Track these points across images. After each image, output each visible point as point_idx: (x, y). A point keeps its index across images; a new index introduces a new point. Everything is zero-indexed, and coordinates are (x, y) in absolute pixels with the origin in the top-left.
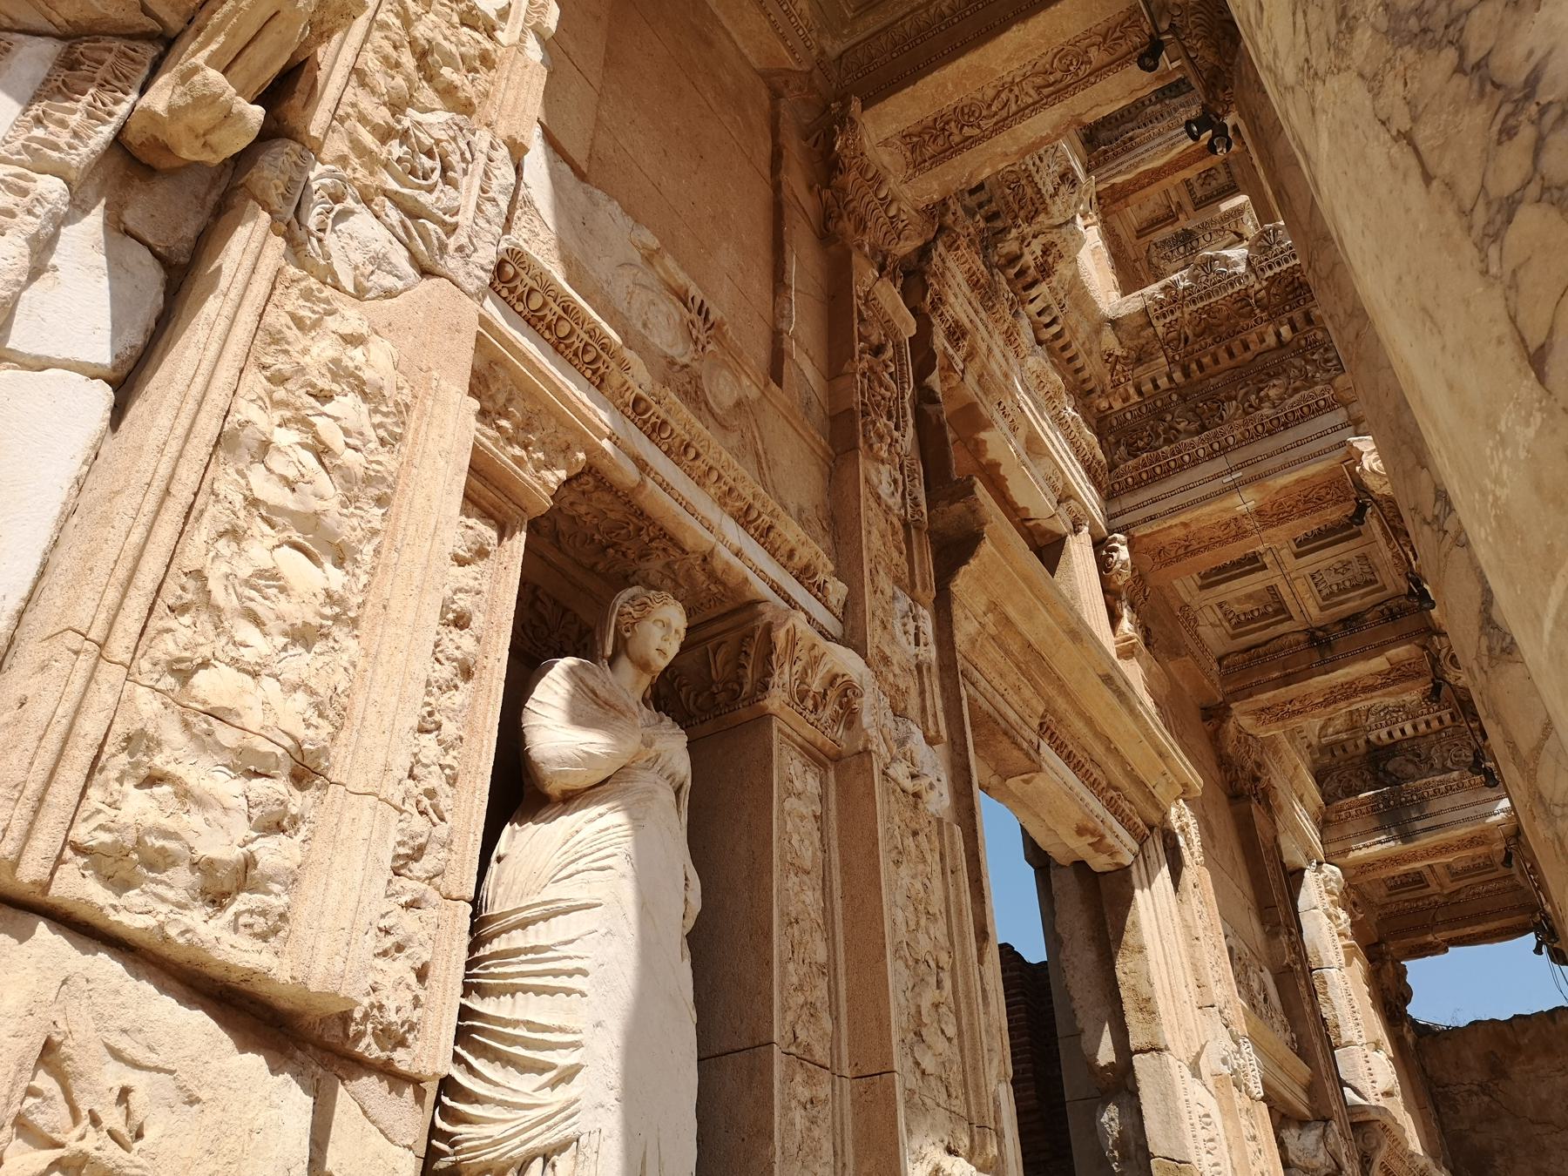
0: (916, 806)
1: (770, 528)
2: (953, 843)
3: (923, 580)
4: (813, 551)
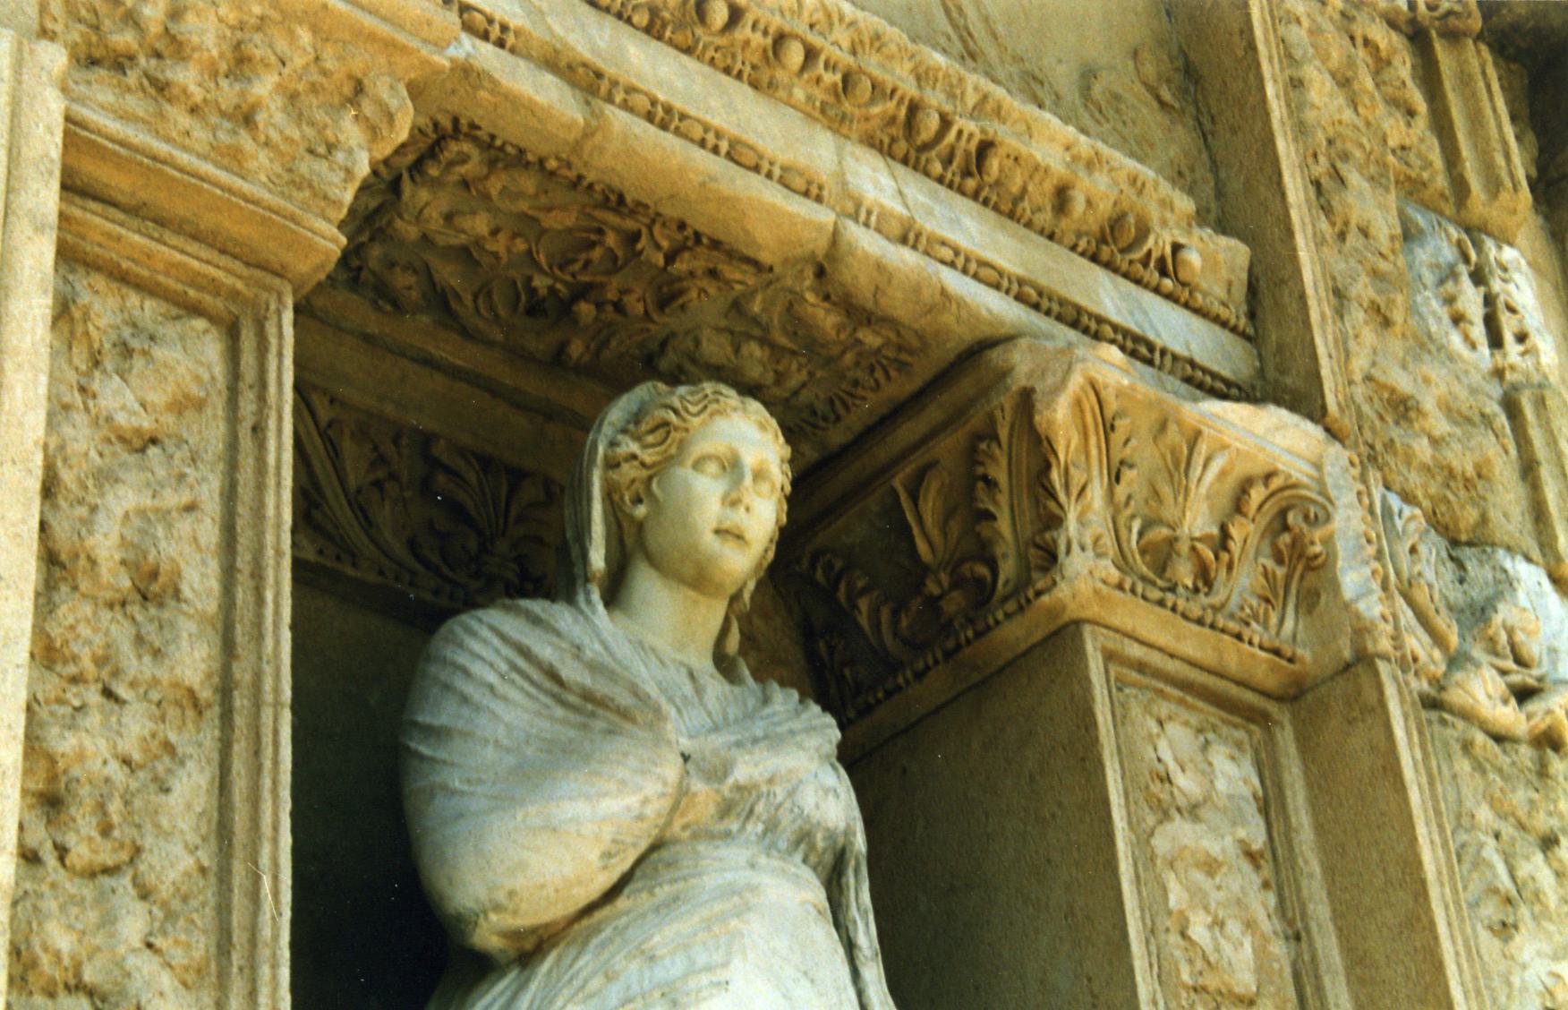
0: (1543, 772)
1: (985, 148)
3: (1488, 170)
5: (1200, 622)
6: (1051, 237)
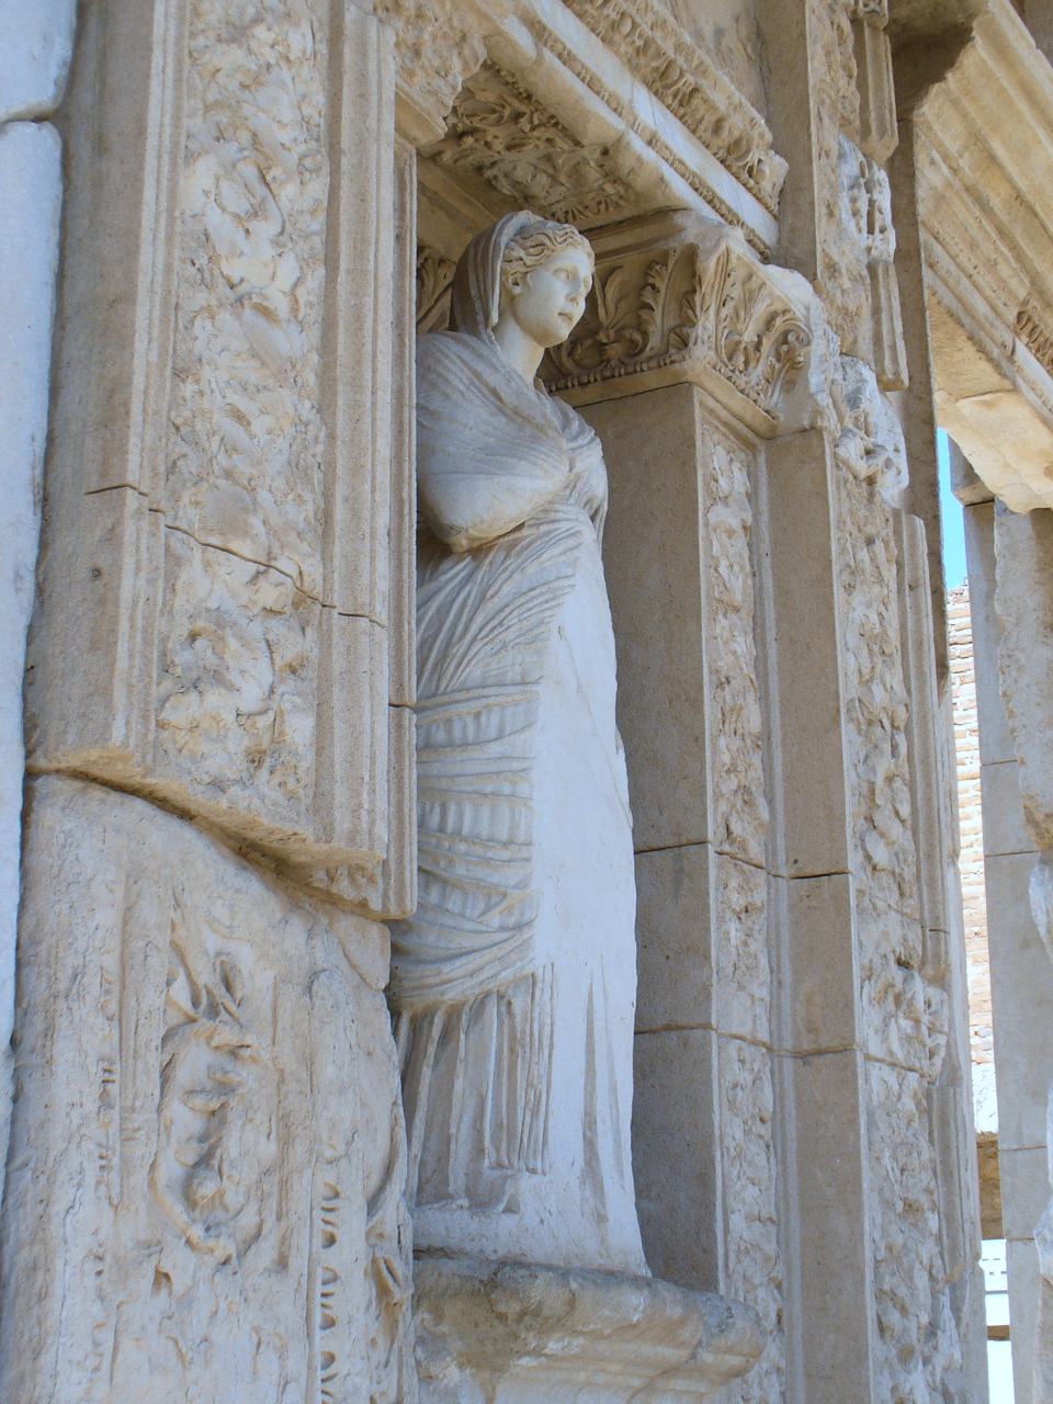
0: (871, 495)
2: (913, 546)
3: (881, 119)
4: (729, 93)
5: (742, 391)
6: (707, 147)
